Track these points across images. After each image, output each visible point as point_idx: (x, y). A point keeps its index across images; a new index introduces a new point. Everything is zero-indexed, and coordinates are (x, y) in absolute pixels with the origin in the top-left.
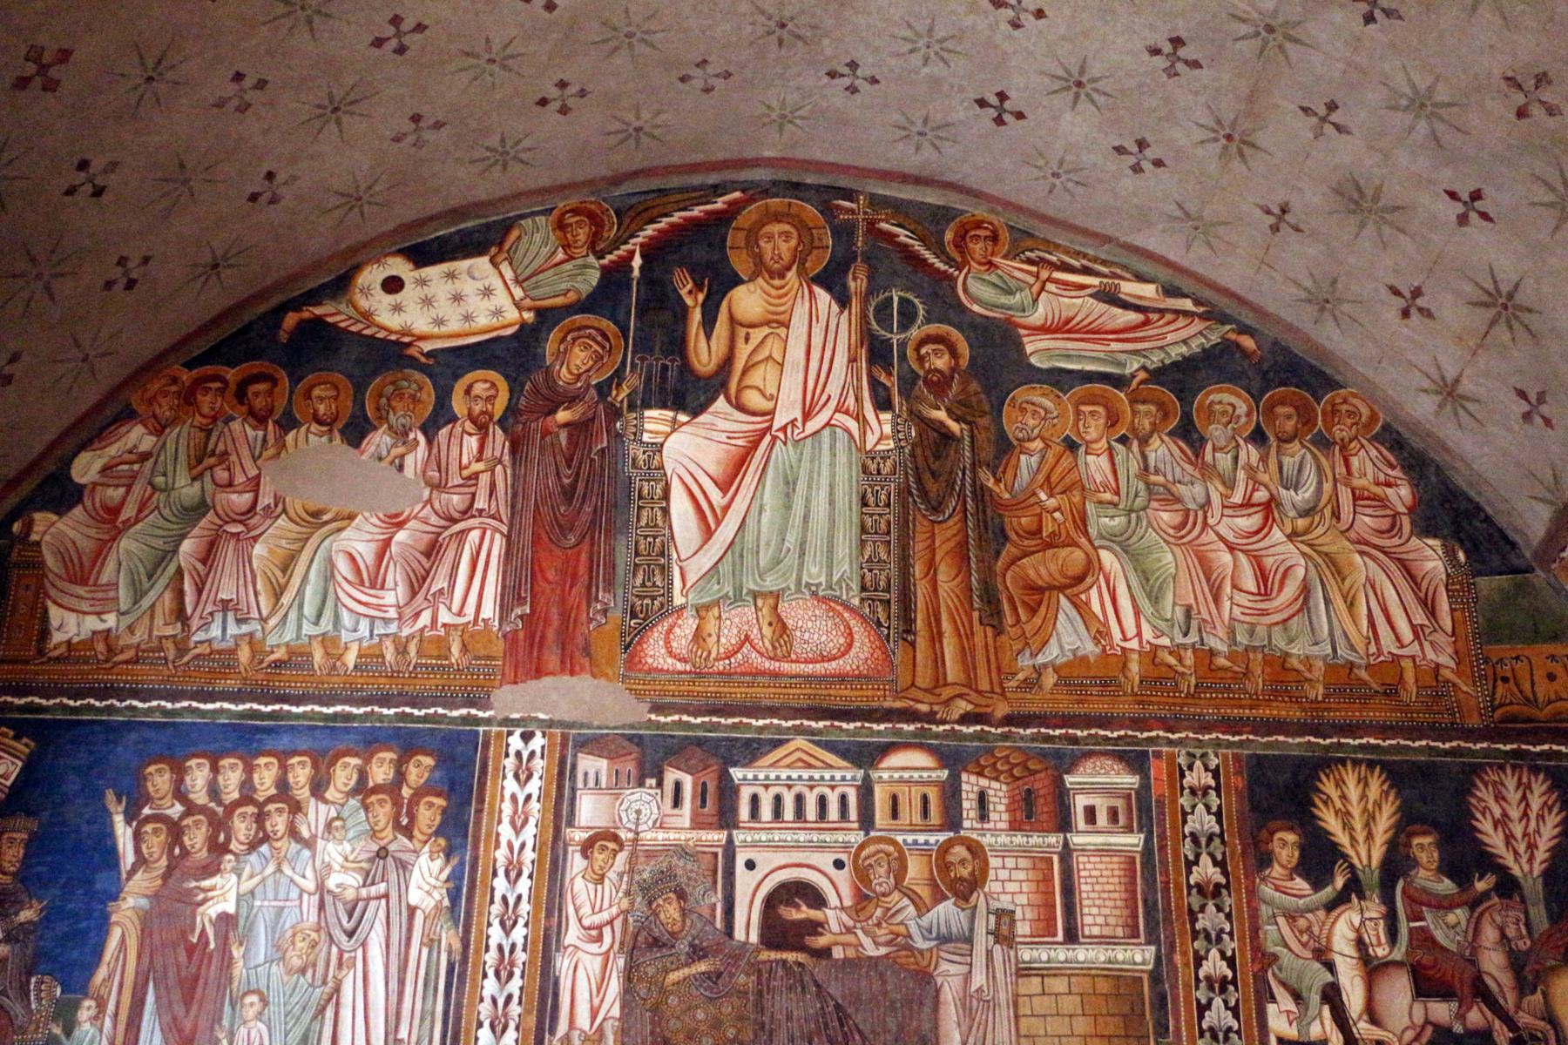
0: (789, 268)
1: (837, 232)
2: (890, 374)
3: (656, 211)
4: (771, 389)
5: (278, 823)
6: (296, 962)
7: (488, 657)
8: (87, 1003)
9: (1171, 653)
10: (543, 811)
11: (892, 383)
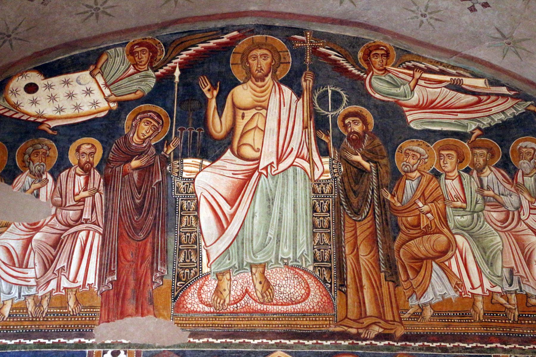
0: (267, 75)
1: (294, 54)
2: (327, 135)
3: (187, 44)
4: (258, 146)
7: (91, 307)
9: (502, 296)
11: (329, 140)
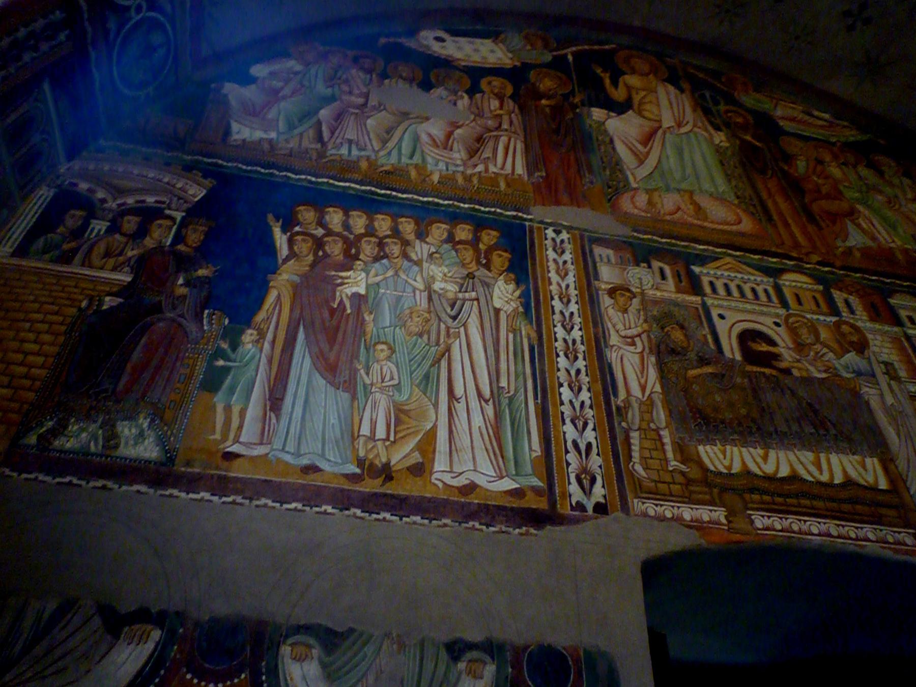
5: (395, 249)
8: (250, 331)
10: (577, 270)
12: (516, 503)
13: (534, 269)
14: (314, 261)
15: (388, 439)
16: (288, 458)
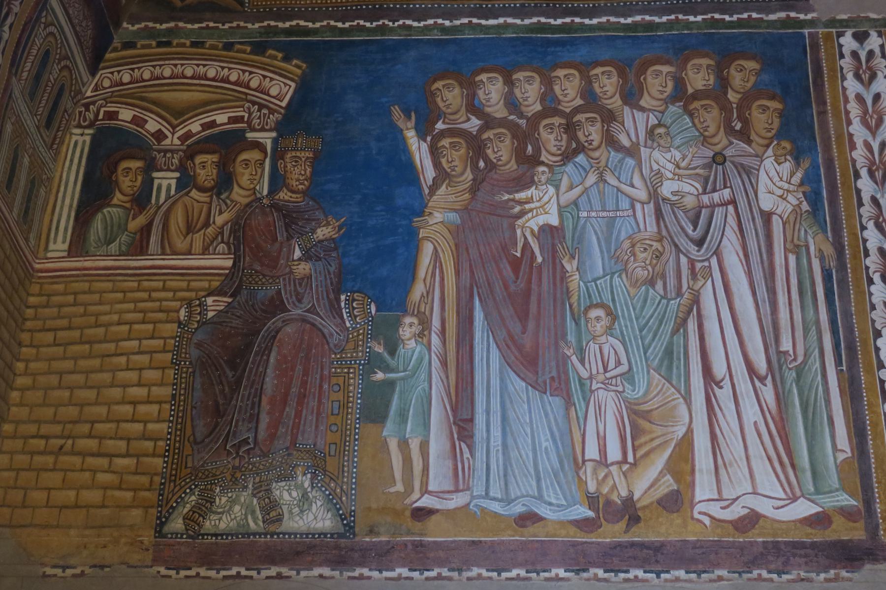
5: (593, 132)
6: (641, 273)
8: (408, 320)
12: (818, 536)
13: (824, 124)
14: (473, 180)
15: (625, 460)
16: (496, 507)
